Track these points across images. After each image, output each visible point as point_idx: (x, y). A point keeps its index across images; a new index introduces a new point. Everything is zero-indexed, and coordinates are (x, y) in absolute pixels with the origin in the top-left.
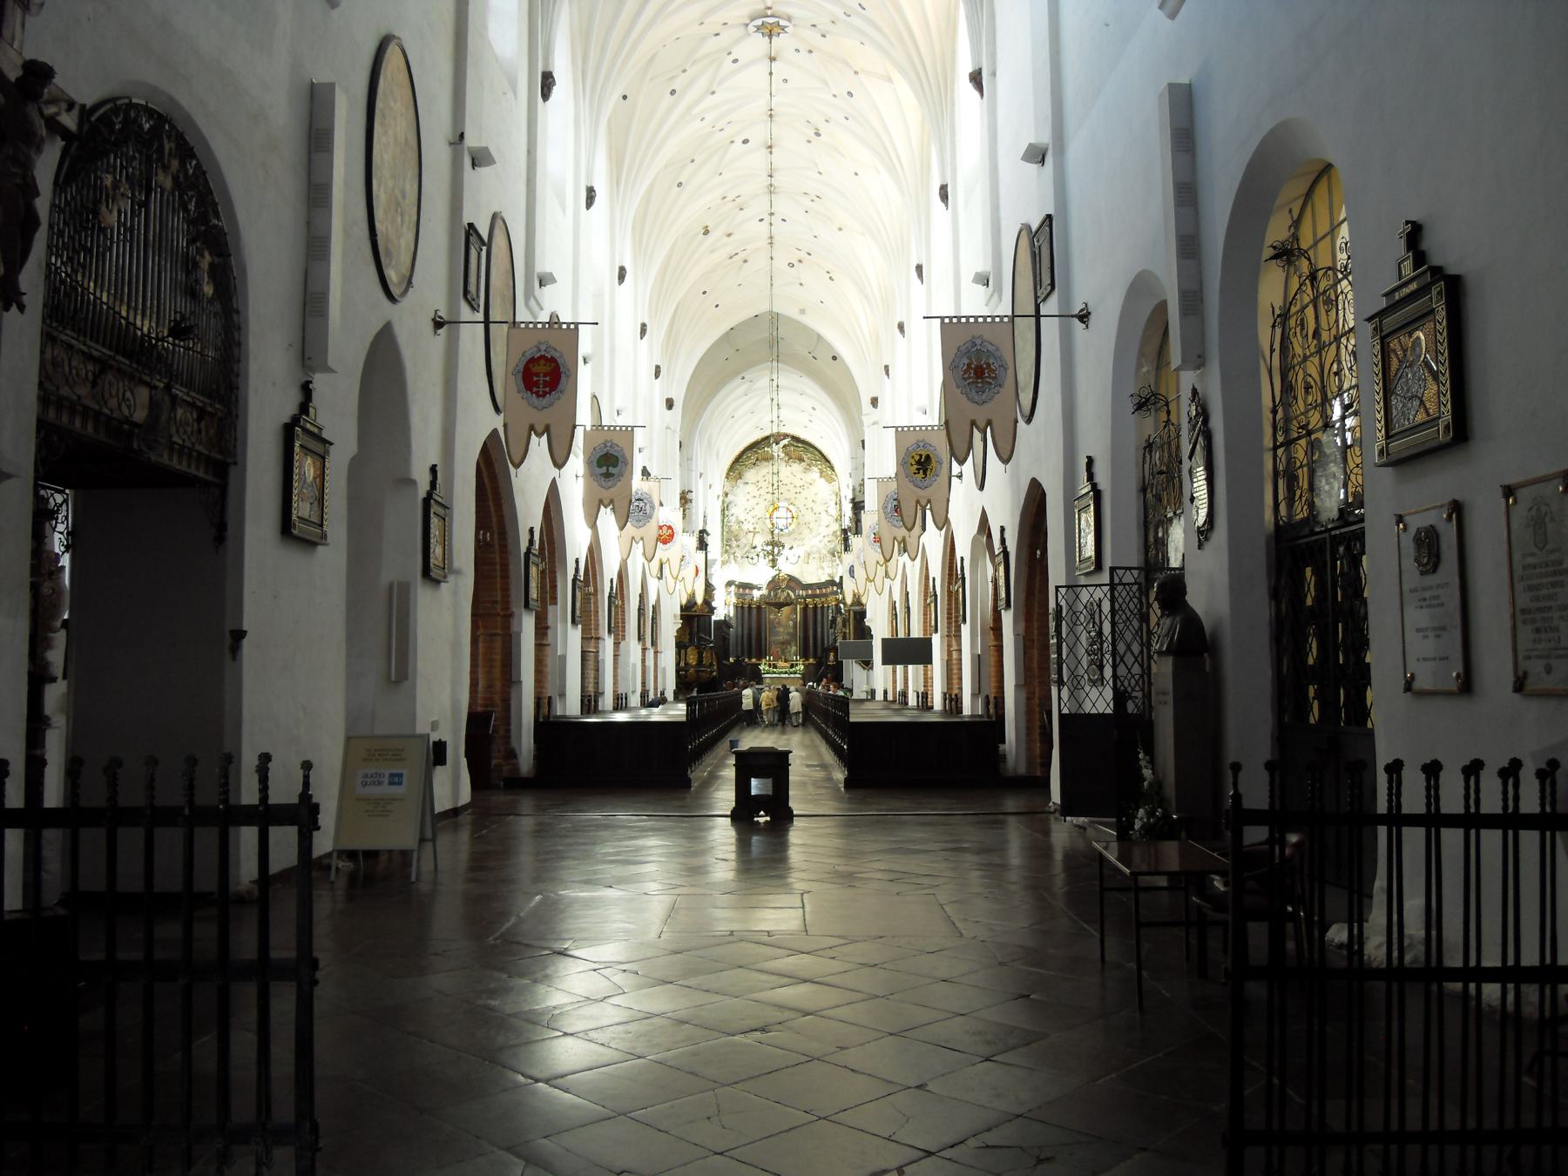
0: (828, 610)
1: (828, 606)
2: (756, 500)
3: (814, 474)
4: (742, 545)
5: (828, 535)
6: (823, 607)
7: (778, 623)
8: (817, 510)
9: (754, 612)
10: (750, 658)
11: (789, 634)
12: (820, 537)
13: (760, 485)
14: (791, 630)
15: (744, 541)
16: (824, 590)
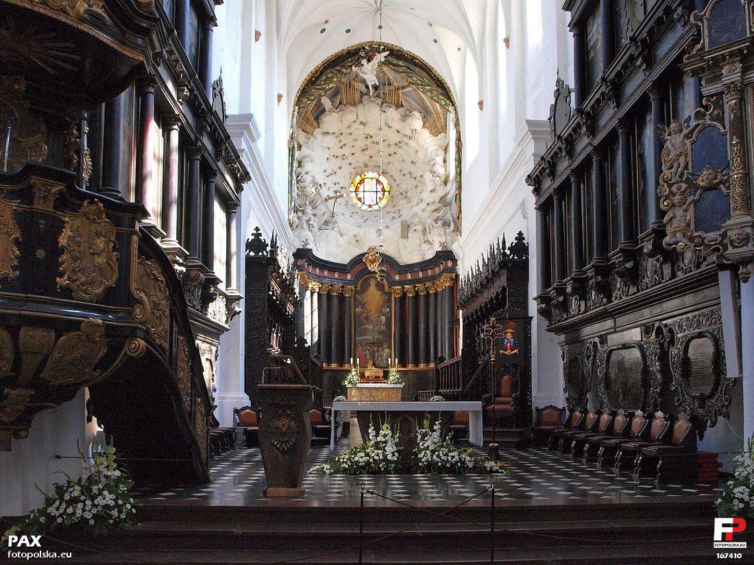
0: (436, 298)
1: (436, 294)
2: (339, 162)
3: (417, 122)
4: (319, 212)
5: (434, 203)
6: (427, 296)
7: (367, 318)
8: (417, 173)
9: (335, 302)
10: (329, 363)
11: (381, 333)
12: (423, 206)
13: (345, 139)
14: (383, 328)
15: (322, 208)
16: (430, 272)
